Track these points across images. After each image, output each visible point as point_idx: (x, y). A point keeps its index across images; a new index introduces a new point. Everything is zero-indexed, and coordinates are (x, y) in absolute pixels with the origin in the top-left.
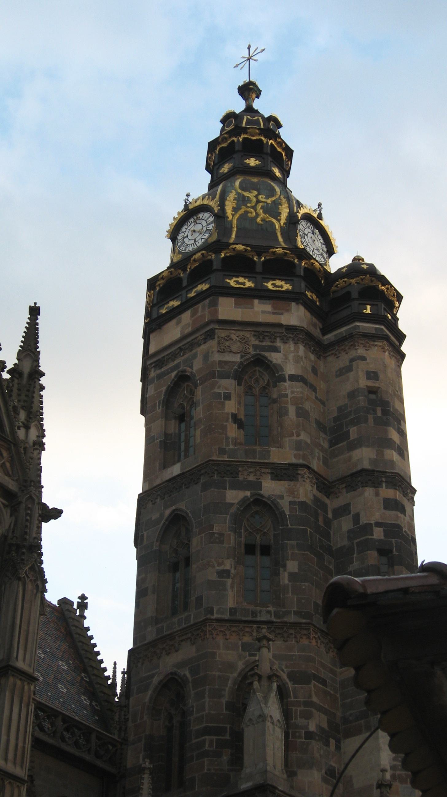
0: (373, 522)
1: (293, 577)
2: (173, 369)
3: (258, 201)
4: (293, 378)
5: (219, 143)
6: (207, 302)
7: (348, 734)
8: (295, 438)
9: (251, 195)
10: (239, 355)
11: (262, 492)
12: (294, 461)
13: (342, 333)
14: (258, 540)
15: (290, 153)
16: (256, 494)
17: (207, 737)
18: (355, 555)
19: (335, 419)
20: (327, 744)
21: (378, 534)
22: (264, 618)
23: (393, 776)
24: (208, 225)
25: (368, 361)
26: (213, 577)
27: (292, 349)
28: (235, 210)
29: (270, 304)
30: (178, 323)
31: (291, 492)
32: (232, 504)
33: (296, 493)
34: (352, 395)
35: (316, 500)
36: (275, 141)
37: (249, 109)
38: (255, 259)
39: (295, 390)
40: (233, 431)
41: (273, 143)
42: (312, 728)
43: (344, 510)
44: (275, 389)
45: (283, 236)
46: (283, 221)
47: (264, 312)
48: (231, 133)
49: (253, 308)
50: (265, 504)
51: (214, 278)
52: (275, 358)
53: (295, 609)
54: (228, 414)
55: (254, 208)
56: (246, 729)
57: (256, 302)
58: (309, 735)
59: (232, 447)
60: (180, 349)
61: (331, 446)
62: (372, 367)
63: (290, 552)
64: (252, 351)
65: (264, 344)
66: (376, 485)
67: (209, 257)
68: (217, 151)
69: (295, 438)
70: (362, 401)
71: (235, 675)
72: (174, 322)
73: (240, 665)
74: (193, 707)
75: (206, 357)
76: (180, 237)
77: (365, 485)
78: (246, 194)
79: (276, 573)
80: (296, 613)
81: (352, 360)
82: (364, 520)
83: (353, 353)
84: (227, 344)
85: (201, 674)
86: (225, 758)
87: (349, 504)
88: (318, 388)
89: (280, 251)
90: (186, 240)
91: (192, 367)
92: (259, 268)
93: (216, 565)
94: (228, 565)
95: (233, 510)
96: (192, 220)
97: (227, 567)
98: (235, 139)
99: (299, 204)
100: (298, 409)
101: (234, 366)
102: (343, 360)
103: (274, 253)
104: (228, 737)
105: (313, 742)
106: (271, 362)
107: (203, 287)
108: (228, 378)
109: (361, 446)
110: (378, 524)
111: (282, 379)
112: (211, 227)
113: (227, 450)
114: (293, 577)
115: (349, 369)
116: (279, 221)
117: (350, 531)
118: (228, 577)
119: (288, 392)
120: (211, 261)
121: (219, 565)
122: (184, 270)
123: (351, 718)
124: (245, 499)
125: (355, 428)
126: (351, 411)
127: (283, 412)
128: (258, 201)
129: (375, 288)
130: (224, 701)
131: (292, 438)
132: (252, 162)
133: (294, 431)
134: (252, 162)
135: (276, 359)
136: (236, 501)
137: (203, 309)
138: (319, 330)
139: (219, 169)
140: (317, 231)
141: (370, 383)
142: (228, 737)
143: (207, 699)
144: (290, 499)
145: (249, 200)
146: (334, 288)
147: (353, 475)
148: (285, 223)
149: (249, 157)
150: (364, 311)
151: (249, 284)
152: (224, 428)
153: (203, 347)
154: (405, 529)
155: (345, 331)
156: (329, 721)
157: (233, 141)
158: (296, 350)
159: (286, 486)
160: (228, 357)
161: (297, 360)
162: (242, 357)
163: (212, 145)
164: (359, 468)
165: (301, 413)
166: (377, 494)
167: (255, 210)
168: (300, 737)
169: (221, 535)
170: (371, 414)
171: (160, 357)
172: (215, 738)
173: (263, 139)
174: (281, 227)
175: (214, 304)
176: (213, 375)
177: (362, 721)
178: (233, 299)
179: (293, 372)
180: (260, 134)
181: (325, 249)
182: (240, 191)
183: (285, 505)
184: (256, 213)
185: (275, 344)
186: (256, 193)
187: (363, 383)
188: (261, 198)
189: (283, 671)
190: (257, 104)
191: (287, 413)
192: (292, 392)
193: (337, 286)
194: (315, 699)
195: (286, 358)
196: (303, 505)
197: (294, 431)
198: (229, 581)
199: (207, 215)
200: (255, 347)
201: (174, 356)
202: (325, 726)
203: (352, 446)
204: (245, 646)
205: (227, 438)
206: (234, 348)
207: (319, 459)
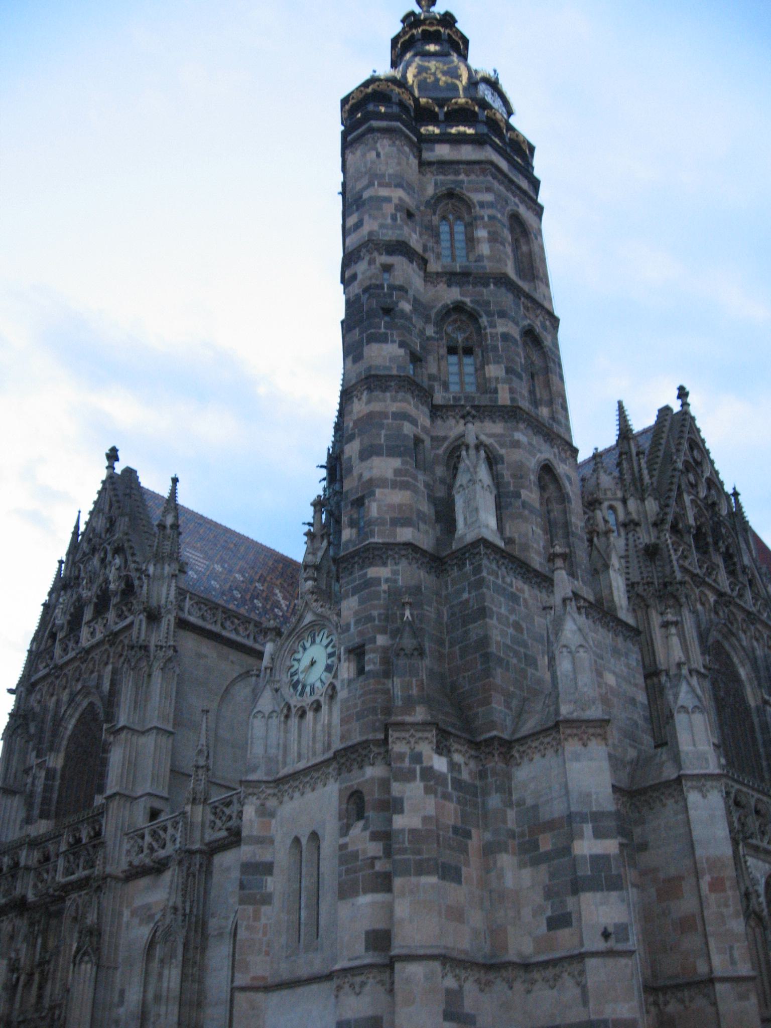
5: (401, 37)
15: (466, 42)
36: (451, 30)
38: (437, 109)
41: (450, 33)
68: (399, 46)
89: (462, 101)
92: (441, 117)
99: (476, 71)
103: (456, 103)
134: (432, 48)
140: (496, 94)
145: (428, 68)
149: (428, 43)
157: (413, 35)
163: (395, 41)
180: (438, 25)
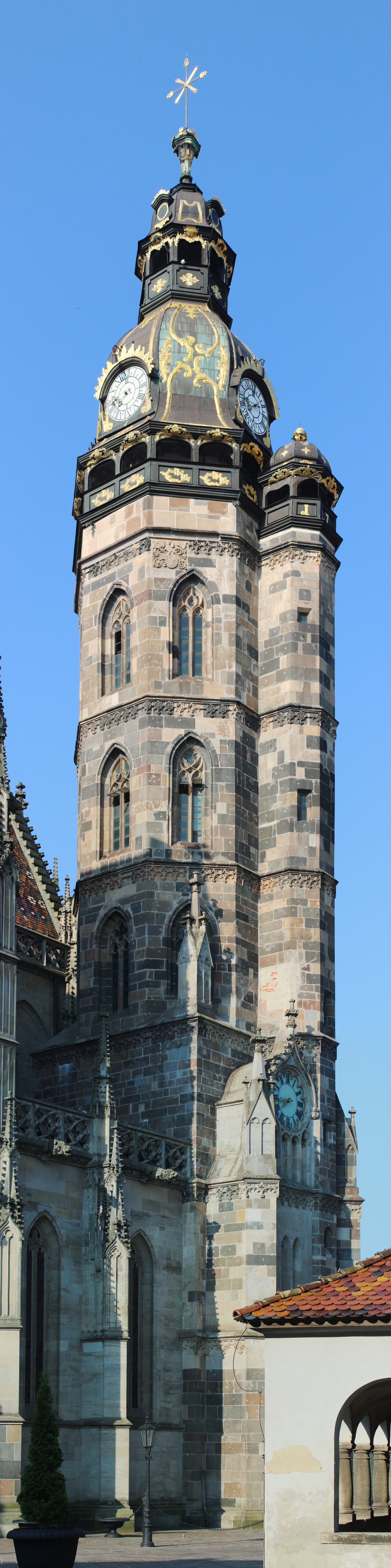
0: (296, 762)
3: (195, 354)
4: (226, 599)
8: (227, 669)
9: (186, 343)
10: (174, 571)
11: (195, 731)
13: (277, 539)
16: (189, 733)
17: (148, 970)
18: (278, 795)
23: (300, 1004)
24: (141, 387)
25: (302, 576)
27: (227, 563)
29: (206, 505)
31: (222, 730)
32: (168, 743)
33: (226, 731)
39: (229, 613)
44: (210, 610)
45: (220, 406)
47: (200, 515)
49: (189, 511)
53: (223, 851)
54: (163, 642)
55: (191, 363)
56: (179, 966)
59: (167, 680)
63: (220, 793)
65: (199, 556)
67: (143, 440)
69: (227, 669)
71: (171, 913)
73: (175, 905)
74: (135, 941)
75: (141, 572)
84: (162, 556)
85: (142, 912)
86: (162, 987)
87: (275, 740)
88: (251, 607)
91: (127, 581)
93: (153, 807)
95: (169, 749)
98: (169, 240)
101: (169, 584)
104: (164, 970)
106: (206, 579)
108: (163, 599)
110: (301, 764)
113: (163, 683)
114: (222, 818)
116: (217, 382)
118: (164, 818)
119: (222, 616)
121: (156, 807)
123: (267, 950)
125: (285, 656)
126: (282, 636)
128: (195, 354)
130: (162, 936)
131: (225, 670)
133: (227, 662)
135: (211, 576)
138: (255, 533)
141: (303, 605)
142: (164, 970)
143: (147, 936)
144: (222, 738)
148: (224, 386)
150: (302, 513)
154: (326, 767)
155: (282, 537)
158: (231, 564)
159: (218, 724)
162: (177, 573)
166: (301, 732)
167: (192, 367)
168: (224, 969)
169: (158, 775)
170: (300, 641)
172: (154, 970)
173: (201, 240)
174: (219, 391)
175: (149, 506)
177: (277, 953)
178: (168, 498)
179: (227, 593)
181: (266, 414)
182: (175, 337)
184: (193, 372)
185: (210, 557)
186: (192, 339)
189: (211, 909)
192: (226, 616)
193: (275, 477)
195: (221, 574)
197: (227, 662)
200: (191, 560)
202: (245, 958)
204: (179, 887)
206: (170, 564)
207: (249, 691)
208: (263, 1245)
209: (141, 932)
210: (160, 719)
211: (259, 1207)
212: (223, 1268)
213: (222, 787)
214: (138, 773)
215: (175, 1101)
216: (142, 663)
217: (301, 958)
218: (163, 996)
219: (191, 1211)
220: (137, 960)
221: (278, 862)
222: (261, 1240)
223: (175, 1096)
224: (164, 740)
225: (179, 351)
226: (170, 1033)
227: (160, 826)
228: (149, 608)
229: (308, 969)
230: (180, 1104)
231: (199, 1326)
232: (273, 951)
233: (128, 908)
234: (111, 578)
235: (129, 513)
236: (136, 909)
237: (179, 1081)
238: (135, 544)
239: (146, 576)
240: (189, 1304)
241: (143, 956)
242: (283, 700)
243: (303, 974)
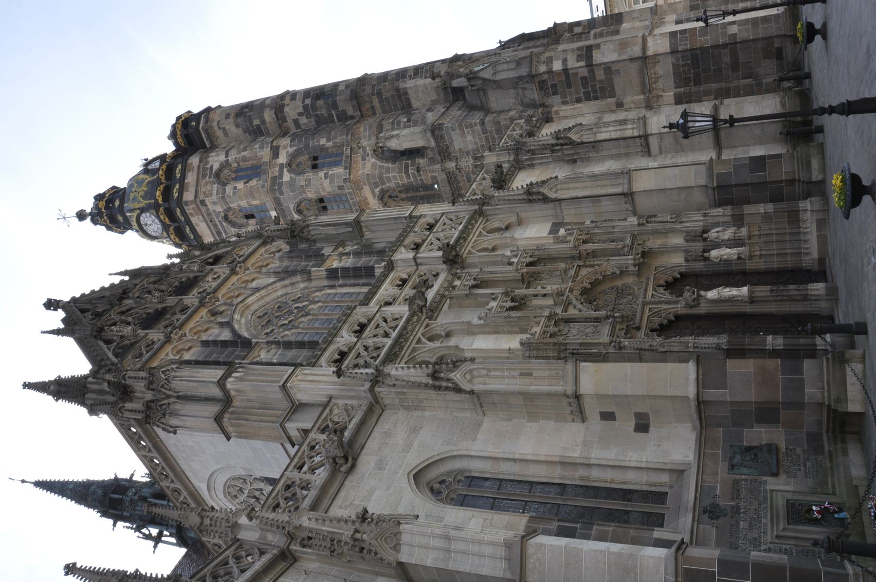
1: (328, 140)
2: (222, 225)
3: (136, 191)
4: (227, 156)
6: (186, 208)
7: (410, 106)
12: (269, 149)
14: (310, 163)
17: (410, 171)
19: (250, 135)
20: (414, 113)
21: (308, 101)
22: (349, 151)
26: (328, 181)
28: (139, 202)
30: (198, 225)
34: (237, 126)
35: (290, 136)
37: (90, 214)
40: (253, 182)
42: (405, 120)
43: (296, 122)
46: (147, 177)
48: (101, 217)
50: (291, 160)
51: (173, 204)
52: (216, 166)
57: (186, 181)
58: (409, 120)
60: (211, 221)
61: (264, 135)
62: (223, 117)
64: (211, 179)
66: (283, 106)
70: (240, 120)
71: (378, 162)
72: (196, 228)
73: (373, 160)
75: (214, 203)
76: (154, 234)
77: (283, 112)
78: (131, 198)
79: (327, 148)
80: (347, 136)
81: (220, 128)
82: (301, 110)
83: (216, 128)
90: (155, 230)
94: (321, 174)
95: (293, 176)
96: (145, 228)
97: (323, 174)
100: (243, 151)
102: (220, 133)
105: (412, 118)
107: (178, 211)
109: (263, 117)
110: (303, 102)
111: (227, 161)
112: (148, 214)
115: (224, 129)
117: (307, 118)
118: (328, 173)
119: (234, 157)
120: (165, 209)
122: (170, 226)
124: (288, 171)
127: (244, 159)
129: (183, 122)
130: (391, 166)
132: (117, 203)
134: (117, 203)
136: (289, 175)
137: (189, 209)
139: (121, 223)
142: (410, 161)
146: (183, 145)
147: (278, 119)
151: (177, 186)
152: (251, 187)
153: (209, 206)
156: (403, 114)
158: (213, 156)
160: (215, 192)
161: (218, 155)
164: (274, 116)
165: (245, 149)
166: (288, 105)
171: (215, 234)
175: (187, 203)
176: (223, 198)
179: (224, 156)
183: (291, 150)
187: (231, 120)
188: (133, 190)
190: (88, 211)
191: (245, 156)
194: (391, 121)
196: (291, 141)
198: (330, 172)
199: (142, 218)
200: (210, 177)
201: (215, 225)
203: (263, 122)
205: (256, 185)
208: (578, 56)
209: (388, 179)
210: (279, 183)
211: (552, 63)
212: (598, 86)
213: (313, 143)
214: (305, 193)
215: (487, 138)
216: (254, 198)
217: (404, 81)
218: (425, 160)
219: (559, 114)
220: (405, 181)
221: (353, 106)
222: (575, 58)
223: (484, 138)
224: (288, 179)
225: (135, 199)
226: (445, 148)
227: (331, 175)
228: (229, 196)
229: (410, 76)
230: (489, 134)
231: (642, 97)
232: (401, 101)
233: (377, 190)
234: (220, 222)
235: (192, 214)
236: (376, 185)
237: (474, 137)
238: (203, 209)
239: (215, 200)
240: (625, 107)
241: (402, 176)
242: (273, 118)
243: (414, 78)
